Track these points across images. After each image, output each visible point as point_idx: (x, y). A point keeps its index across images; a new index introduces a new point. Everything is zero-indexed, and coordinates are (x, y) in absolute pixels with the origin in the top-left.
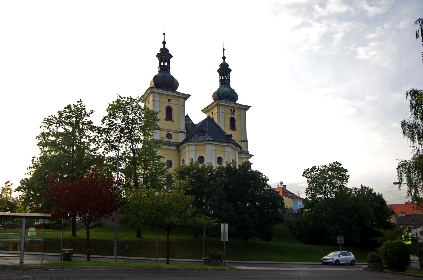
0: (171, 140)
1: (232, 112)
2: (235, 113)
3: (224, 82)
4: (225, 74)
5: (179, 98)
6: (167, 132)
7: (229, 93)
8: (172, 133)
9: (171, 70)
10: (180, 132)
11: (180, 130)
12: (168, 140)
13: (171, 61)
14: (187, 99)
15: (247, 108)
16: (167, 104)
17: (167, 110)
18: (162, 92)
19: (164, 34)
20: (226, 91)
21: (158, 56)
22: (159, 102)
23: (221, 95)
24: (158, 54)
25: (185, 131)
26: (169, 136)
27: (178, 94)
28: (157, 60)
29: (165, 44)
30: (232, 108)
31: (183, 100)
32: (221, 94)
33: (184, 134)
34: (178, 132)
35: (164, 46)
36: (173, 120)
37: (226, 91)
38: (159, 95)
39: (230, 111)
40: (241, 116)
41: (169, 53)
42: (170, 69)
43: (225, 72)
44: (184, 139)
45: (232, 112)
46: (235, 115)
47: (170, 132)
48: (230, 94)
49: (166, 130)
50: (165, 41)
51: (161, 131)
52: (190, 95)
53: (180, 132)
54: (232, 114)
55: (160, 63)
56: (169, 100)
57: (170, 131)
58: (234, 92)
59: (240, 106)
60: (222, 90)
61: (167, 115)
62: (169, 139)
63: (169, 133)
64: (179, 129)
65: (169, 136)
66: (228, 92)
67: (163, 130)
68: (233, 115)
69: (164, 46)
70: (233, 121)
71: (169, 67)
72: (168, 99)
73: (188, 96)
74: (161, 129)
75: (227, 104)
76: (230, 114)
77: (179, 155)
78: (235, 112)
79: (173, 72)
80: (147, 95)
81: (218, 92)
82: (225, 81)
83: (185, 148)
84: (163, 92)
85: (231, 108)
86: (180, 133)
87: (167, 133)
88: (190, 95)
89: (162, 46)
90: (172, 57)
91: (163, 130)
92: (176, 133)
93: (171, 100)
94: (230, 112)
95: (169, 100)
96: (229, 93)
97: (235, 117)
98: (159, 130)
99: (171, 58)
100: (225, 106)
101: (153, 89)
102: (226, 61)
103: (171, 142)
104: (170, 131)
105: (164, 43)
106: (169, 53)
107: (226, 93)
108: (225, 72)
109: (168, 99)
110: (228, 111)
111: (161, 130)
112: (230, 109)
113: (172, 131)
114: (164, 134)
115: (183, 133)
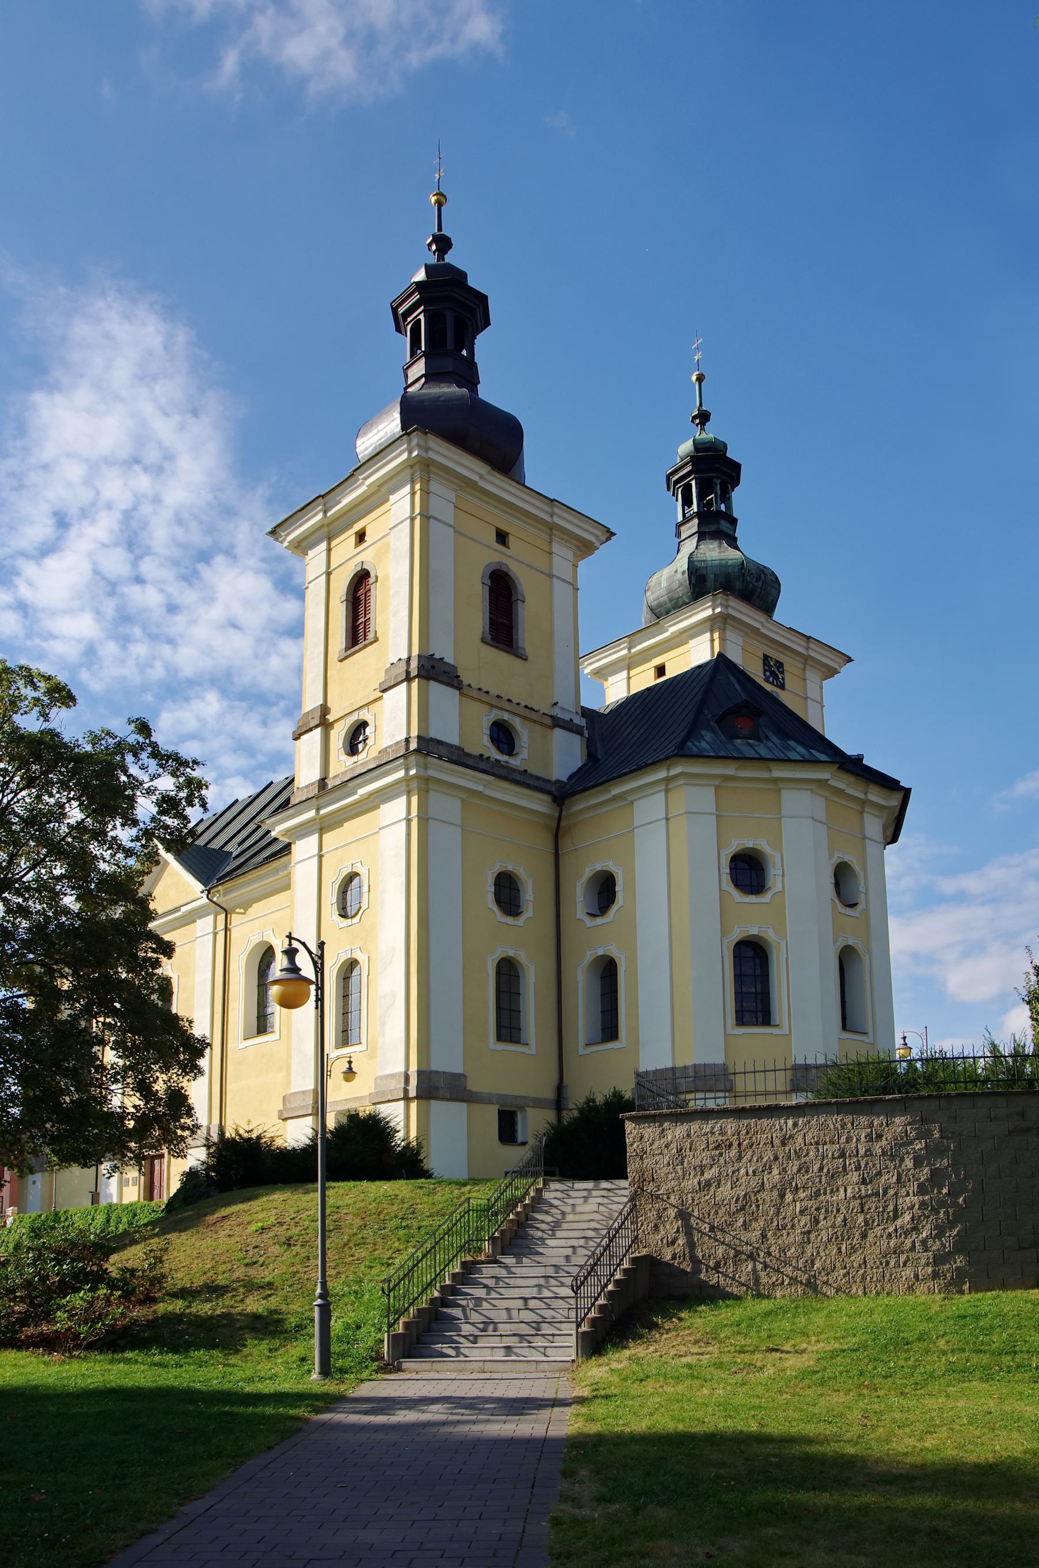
0: (515, 762)
3: (713, 528)
4: (718, 486)
6: (495, 711)
7: (757, 581)
8: (517, 723)
10: (557, 723)
11: (556, 712)
18: (476, 478)
20: (743, 564)
22: (457, 532)
32: (712, 576)
33: (579, 737)
37: (743, 564)
40: (806, 698)
44: (580, 765)
46: (782, 687)
48: (760, 584)
49: (497, 702)
51: (465, 699)
53: (557, 723)
54: (773, 684)
57: (508, 706)
58: (774, 579)
59: (807, 649)
61: (490, 619)
62: (502, 752)
63: (506, 716)
66: (753, 571)
67: (475, 694)
68: (777, 686)
74: (465, 690)
82: (719, 523)
83: (632, 803)
84: (481, 477)
85: (771, 653)
86: (558, 731)
91: (475, 694)
92: (538, 726)
94: (765, 671)
95: (502, 537)
96: (757, 581)
98: (457, 692)
103: (514, 770)
104: (508, 706)
107: (744, 574)
108: (716, 477)
113: (521, 710)
114: (484, 719)
115: (577, 733)
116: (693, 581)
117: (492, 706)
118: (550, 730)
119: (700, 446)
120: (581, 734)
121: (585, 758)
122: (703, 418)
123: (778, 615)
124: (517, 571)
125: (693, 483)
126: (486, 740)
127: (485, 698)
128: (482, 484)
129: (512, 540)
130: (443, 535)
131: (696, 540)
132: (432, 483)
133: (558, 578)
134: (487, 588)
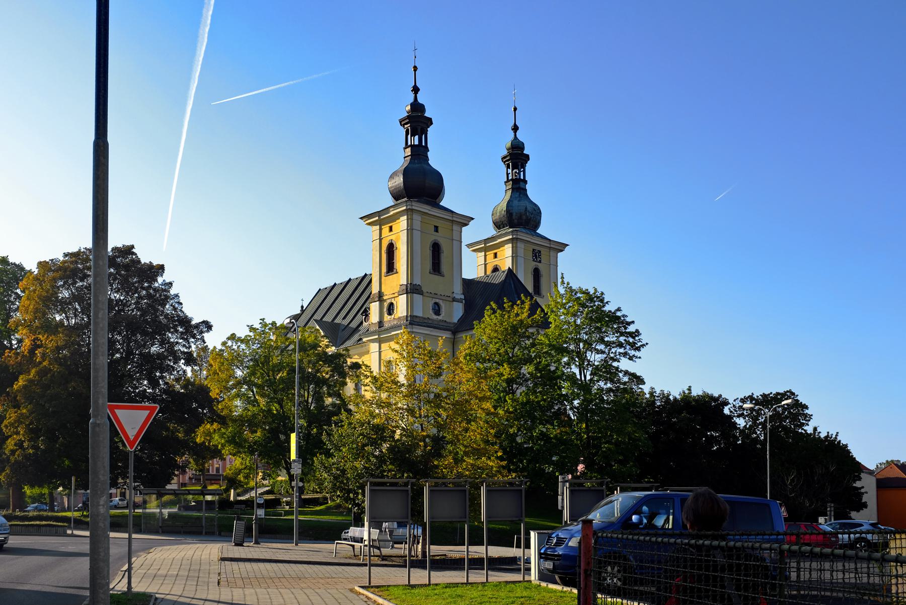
1: (536, 255)
2: (541, 258)
3: (518, 186)
5: (453, 223)
6: (434, 299)
8: (441, 302)
12: (435, 317)
15: (562, 247)
16: (434, 237)
19: (415, 68)
22: (421, 232)
23: (514, 217)
25: (463, 297)
26: (437, 310)
27: (454, 215)
30: (537, 248)
34: (451, 300)
37: (526, 208)
38: (420, 217)
39: (533, 253)
43: (520, 164)
45: (536, 258)
46: (540, 262)
47: (439, 300)
51: (425, 297)
54: (536, 261)
58: (539, 211)
60: (518, 206)
63: (437, 301)
64: (453, 292)
65: (437, 310)
67: (427, 295)
68: (538, 262)
70: (537, 274)
72: (435, 226)
75: (529, 240)
76: (534, 260)
77: (453, 350)
78: (540, 255)
79: (435, 160)
81: (510, 208)
82: (519, 184)
86: (454, 302)
87: (433, 302)
89: (412, 100)
94: (533, 256)
95: (436, 229)
97: (540, 266)
100: (525, 243)
101: (413, 204)
102: (521, 136)
109: (435, 226)
110: (530, 255)
111: (425, 296)
112: (534, 250)
113: (444, 298)
114: (430, 303)
116: (508, 215)
117: (433, 298)
118: (451, 303)
119: (514, 146)
120: (462, 302)
121: (463, 311)
122: (515, 128)
123: (540, 231)
125: (511, 164)
126: (431, 312)
127: (431, 295)
128: (430, 212)
129: (439, 229)
130: (417, 235)
131: (511, 191)
132: (414, 216)
133: (455, 240)
134: (431, 251)
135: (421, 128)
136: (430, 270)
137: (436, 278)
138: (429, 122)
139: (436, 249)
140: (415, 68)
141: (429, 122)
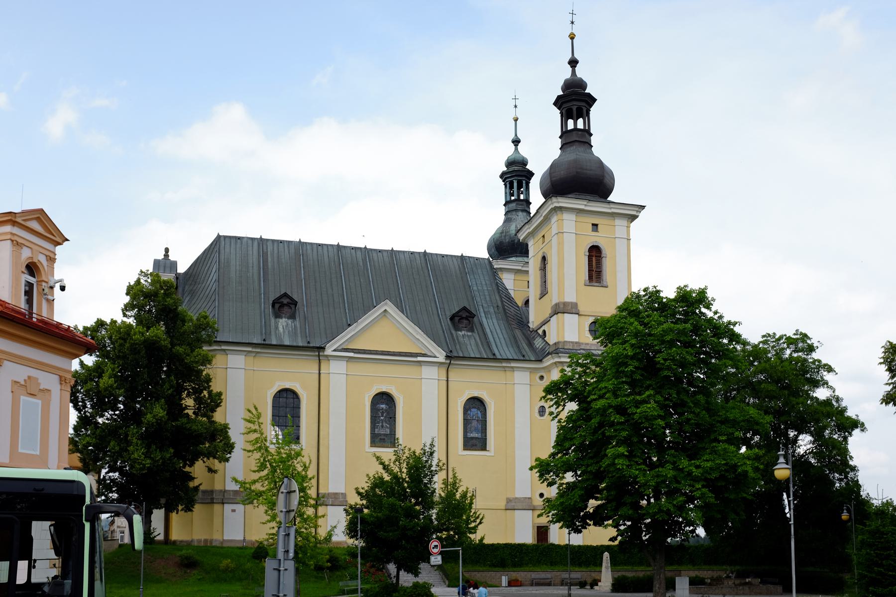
9: (594, 140)
13: (594, 110)
14: (633, 218)
17: (588, 256)
21: (559, 103)
24: (559, 97)
28: (556, 113)
29: (575, 67)
31: (624, 222)
35: (574, 72)
36: (605, 283)
41: (587, 91)
42: (592, 138)
50: (575, 56)
52: (643, 207)
55: (564, 124)
56: (595, 226)
69: (574, 72)
71: (587, 132)
72: (593, 225)
73: (637, 211)
80: (542, 218)
88: (643, 207)
89: (567, 73)
90: (594, 100)
93: (599, 225)
99: (591, 106)
105: (573, 63)
106: (587, 91)
124: (601, 243)
126: (588, 334)
135: (577, 109)
136: (585, 280)
137: (595, 290)
138: (591, 100)
139: (595, 252)
140: (572, 37)
141: (591, 100)
